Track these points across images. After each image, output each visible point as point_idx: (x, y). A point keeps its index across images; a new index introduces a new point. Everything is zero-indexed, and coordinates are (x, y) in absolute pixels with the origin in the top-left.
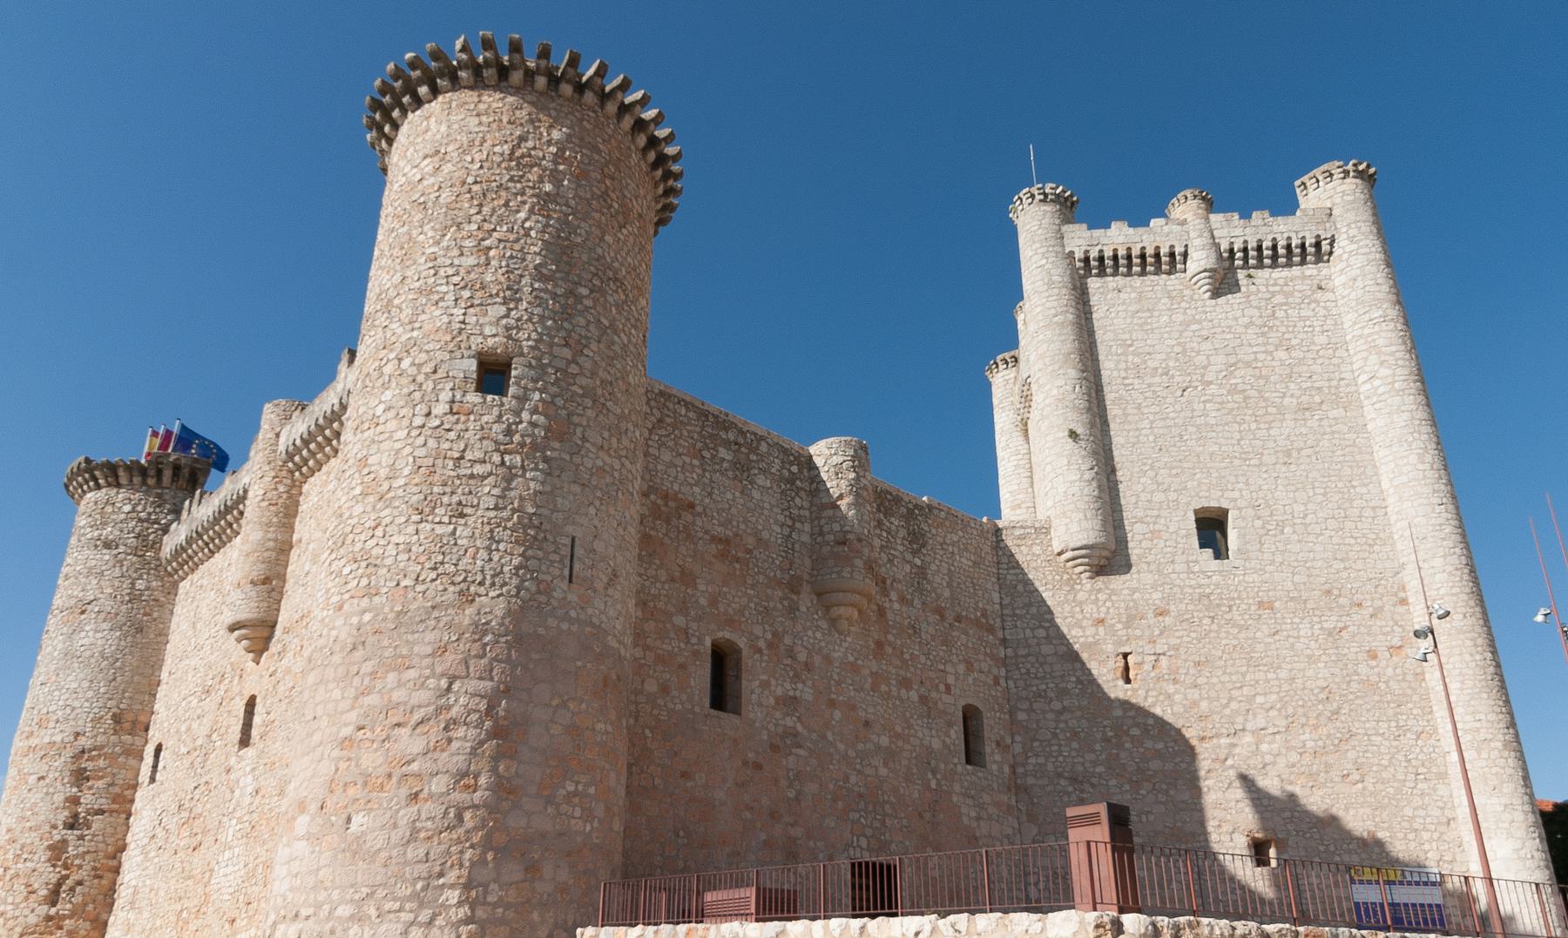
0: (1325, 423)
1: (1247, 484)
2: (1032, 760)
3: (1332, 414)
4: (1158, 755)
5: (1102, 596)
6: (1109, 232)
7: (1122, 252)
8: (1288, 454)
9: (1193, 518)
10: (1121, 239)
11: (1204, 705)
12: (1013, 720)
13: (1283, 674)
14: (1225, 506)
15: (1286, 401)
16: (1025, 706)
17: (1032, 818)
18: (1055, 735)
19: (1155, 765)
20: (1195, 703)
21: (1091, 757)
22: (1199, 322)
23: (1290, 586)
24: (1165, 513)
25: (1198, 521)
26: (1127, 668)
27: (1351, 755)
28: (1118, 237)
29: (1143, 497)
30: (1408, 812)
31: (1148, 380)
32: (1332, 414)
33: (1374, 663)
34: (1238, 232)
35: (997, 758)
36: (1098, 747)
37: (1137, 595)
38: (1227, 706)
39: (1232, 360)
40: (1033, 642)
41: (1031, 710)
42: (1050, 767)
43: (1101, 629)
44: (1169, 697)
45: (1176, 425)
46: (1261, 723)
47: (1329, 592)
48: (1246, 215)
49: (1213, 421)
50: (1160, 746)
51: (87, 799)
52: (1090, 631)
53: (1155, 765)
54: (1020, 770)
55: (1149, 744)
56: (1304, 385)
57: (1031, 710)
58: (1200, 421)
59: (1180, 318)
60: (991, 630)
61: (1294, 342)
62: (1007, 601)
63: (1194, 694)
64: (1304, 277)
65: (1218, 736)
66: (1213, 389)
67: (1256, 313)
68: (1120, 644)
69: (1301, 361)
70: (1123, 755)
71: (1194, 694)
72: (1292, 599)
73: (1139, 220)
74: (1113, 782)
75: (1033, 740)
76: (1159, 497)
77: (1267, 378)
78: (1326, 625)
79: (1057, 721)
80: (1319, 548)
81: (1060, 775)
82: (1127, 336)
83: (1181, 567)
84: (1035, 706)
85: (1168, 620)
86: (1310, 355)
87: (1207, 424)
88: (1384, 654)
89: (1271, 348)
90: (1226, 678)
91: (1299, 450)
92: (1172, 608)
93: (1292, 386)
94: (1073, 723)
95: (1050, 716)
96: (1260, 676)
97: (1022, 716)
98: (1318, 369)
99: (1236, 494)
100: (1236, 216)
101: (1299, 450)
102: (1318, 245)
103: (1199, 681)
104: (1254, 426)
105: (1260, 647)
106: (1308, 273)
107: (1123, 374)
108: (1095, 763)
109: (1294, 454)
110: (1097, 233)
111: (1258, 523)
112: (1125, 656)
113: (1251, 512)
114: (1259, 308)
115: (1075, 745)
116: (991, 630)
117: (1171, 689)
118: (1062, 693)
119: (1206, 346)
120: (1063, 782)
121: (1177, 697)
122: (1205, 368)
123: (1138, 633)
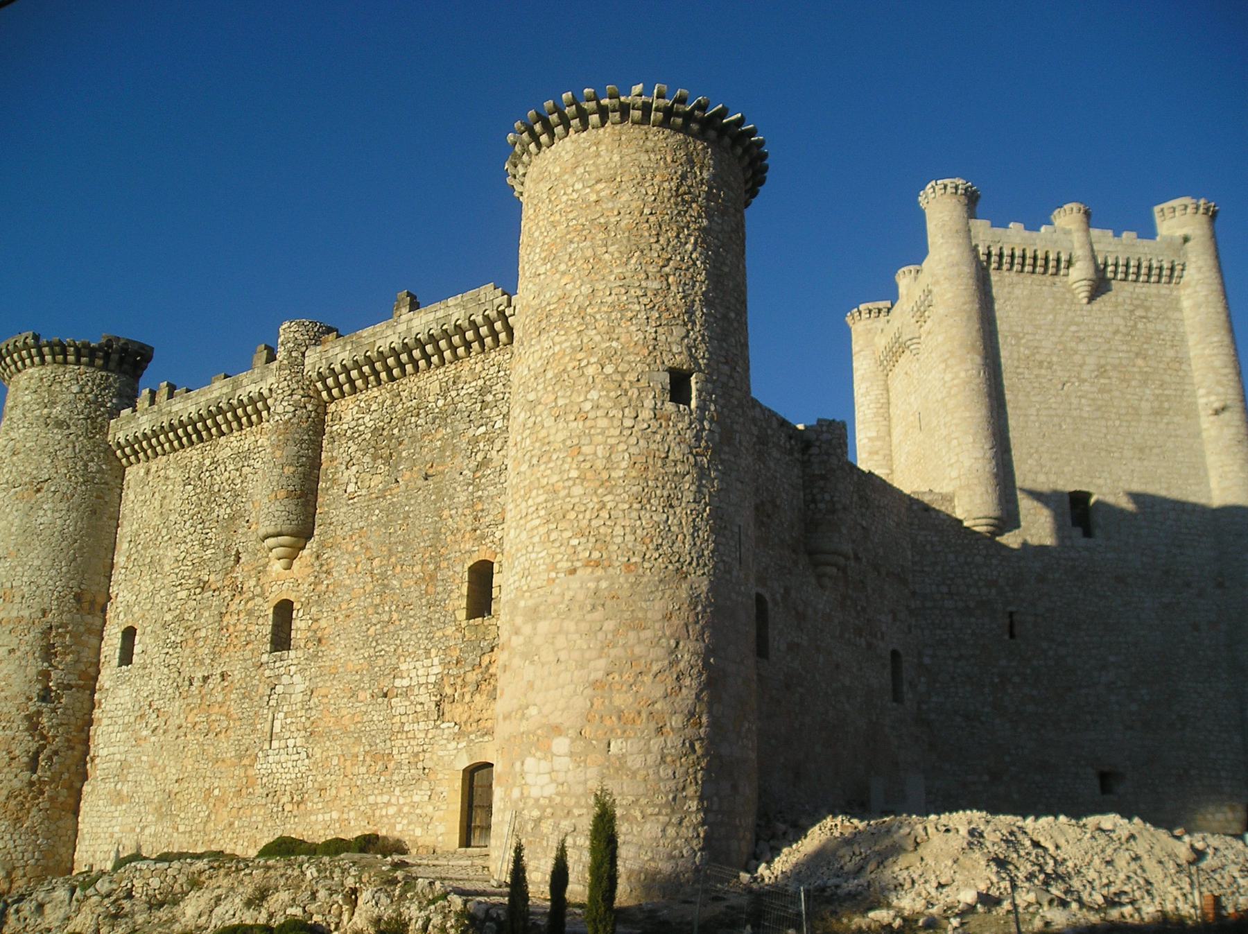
0: (1171, 427)
1: (1110, 473)
2: (934, 699)
3: (1176, 419)
15: (1143, 404)
18: (953, 678)
22: (1077, 324)
26: (1011, 626)
33: (1196, 634)
35: (910, 696)
36: (986, 690)
43: (994, 591)
45: (1057, 415)
49: (1086, 415)
50: (1035, 693)
52: (985, 591)
54: (924, 707)
56: (1157, 392)
58: (1075, 413)
64: (1159, 296)
66: (1086, 387)
73: (1033, 225)
82: (1019, 329)
86: (1161, 366)
87: (1081, 417)
90: (1086, 639)
91: (1151, 448)
92: (1050, 576)
93: (1148, 391)
97: (927, 660)
99: (1101, 482)
100: (1110, 233)
101: (1151, 448)
102: (1172, 269)
104: (1117, 423)
106: (1163, 291)
107: (1016, 363)
109: (1147, 451)
112: (1011, 614)
114: (1124, 318)
117: (1045, 645)
121: (1051, 653)
122: (1081, 366)
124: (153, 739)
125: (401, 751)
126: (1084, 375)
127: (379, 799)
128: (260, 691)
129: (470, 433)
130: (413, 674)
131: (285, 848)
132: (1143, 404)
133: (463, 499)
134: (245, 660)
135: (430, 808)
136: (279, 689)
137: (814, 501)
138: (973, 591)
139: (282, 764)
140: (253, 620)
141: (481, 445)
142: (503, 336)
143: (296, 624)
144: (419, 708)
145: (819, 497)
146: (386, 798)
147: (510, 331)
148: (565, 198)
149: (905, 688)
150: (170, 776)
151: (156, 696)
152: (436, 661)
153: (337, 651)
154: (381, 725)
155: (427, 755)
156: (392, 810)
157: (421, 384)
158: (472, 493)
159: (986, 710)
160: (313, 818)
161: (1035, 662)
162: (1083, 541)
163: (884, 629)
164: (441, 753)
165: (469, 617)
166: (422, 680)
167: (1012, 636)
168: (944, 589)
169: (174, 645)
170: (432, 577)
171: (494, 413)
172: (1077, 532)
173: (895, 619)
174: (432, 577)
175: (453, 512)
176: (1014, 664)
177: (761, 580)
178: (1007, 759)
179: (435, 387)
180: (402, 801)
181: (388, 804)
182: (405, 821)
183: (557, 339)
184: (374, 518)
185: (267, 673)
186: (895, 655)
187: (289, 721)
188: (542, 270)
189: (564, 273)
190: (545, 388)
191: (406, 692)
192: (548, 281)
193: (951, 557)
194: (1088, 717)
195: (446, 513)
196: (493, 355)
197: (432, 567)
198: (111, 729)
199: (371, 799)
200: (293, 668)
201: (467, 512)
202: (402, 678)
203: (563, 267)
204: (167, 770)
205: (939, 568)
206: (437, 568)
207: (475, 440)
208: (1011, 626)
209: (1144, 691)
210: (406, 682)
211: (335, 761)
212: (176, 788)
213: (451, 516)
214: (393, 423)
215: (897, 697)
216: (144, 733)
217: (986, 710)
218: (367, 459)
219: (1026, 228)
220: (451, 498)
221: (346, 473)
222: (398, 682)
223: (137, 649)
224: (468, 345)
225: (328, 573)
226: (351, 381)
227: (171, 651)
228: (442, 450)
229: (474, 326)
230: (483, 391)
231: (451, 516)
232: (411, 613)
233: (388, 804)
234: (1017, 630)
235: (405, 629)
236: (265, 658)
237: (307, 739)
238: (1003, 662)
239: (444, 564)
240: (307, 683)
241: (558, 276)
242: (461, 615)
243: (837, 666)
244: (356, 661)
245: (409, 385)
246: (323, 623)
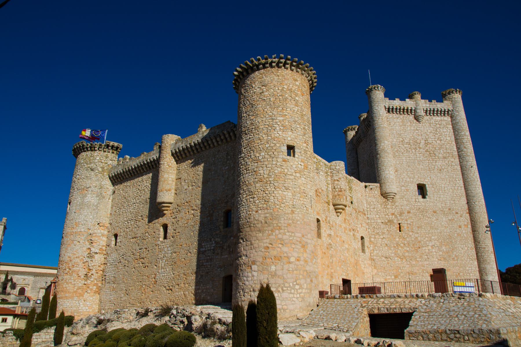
1: (430, 177)
2: (375, 252)
4: (407, 251)
5: (393, 207)
6: (395, 101)
7: (398, 108)
8: (440, 170)
9: (416, 186)
10: (398, 104)
11: (419, 238)
12: (370, 241)
13: (438, 231)
14: (424, 183)
15: (440, 155)
16: (373, 236)
17: (375, 268)
18: (381, 245)
19: (407, 254)
20: (417, 238)
21: (390, 251)
23: (440, 207)
24: (410, 184)
25: (418, 186)
26: (400, 228)
27: (455, 253)
28: (397, 103)
29: (404, 179)
30: (467, 268)
31: (405, 146)
32: (451, 160)
34: (428, 105)
37: (403, 207)
38: (424, 239)
39: (426, 142)
40: (375, 219)
41: (375, 238)
42: (380, 254)
43: (393, 216)
44: (410, 236)
46: (433, 244)
47: (450, 209)
48: (430, 101)
50: (408, 249)
51: (93, 249)
52: (391, 216)
53: (407, 254)
54: (372, 254)
55: (405, 248)
56: (445, 151)
57: (375, 238)
58: (418, 159)
59: (413, 128)
60: (365, 214)
61: (442, 138)
62: (368, 206)
63: (416, 235)
64: (444, 120)
65: (423, 247)
66: (421, 150)
67: (432, 129)
68: (398, 220)
69: (444, 144)
70: (399, 251)
71: (416, 235)
72: (442, 211)
73: (403, 99)
74: (396, 258)
75: (376, 246)
76: (408, 180)
77: (435, 148)
78: (449, 218)
79: (382, 241)
80: (448, 197)
81: (382, 256)
83: (413, 200)
84: (376, 237)
85: (411, 215)
88: (463, 227)
89: (436, 140)
91: (443, 169)
93: (441, 151)
94: (386, 242)
95: (380, 240)
96: (433, 231)
97: (372, 239)
98: (448, 147)
100: (427, 101)
101: (443, 169)
103: (419, 232)
105: (433, 223)
108: (391, 253)
110: (391, 101)
111: (433, 189)
112: (399, 224)
113: (431, 186)
115: (386, 248)
116: (365, 214)
117: (411, 233)
118: (383, 233)
119: (420, 138)
120: (383, 258)
121: (413, 236)
123: (403, 218)
126: (421, 146)
132: (440, 155)
135: (212, 290)
137: (334, 188)
138: (387, 216)
142: (233, 138)
145: (336, 187)
147: (235, 135)
149: (366, 248)
159: (393, 255)
161: (408, 239)
162: (422, 200)
163: (358, 229)
167: (400, 231)
168: (378, 216)
172: (421, 196)
173: (362, 226)
176: (401, 240)
177: (318, 214)
178: (400, 271)
186: (362, 238)
193: (379, 206)
194: (426, 257)
205: (375, 210)
208: (400, 228)
209: (444, 248)
215: (363, 250)
217: (393, 255)
219: (400, 100)
224: (222, 140)
234: (402, 228)
238: (397, 240)
243: (344, 242)
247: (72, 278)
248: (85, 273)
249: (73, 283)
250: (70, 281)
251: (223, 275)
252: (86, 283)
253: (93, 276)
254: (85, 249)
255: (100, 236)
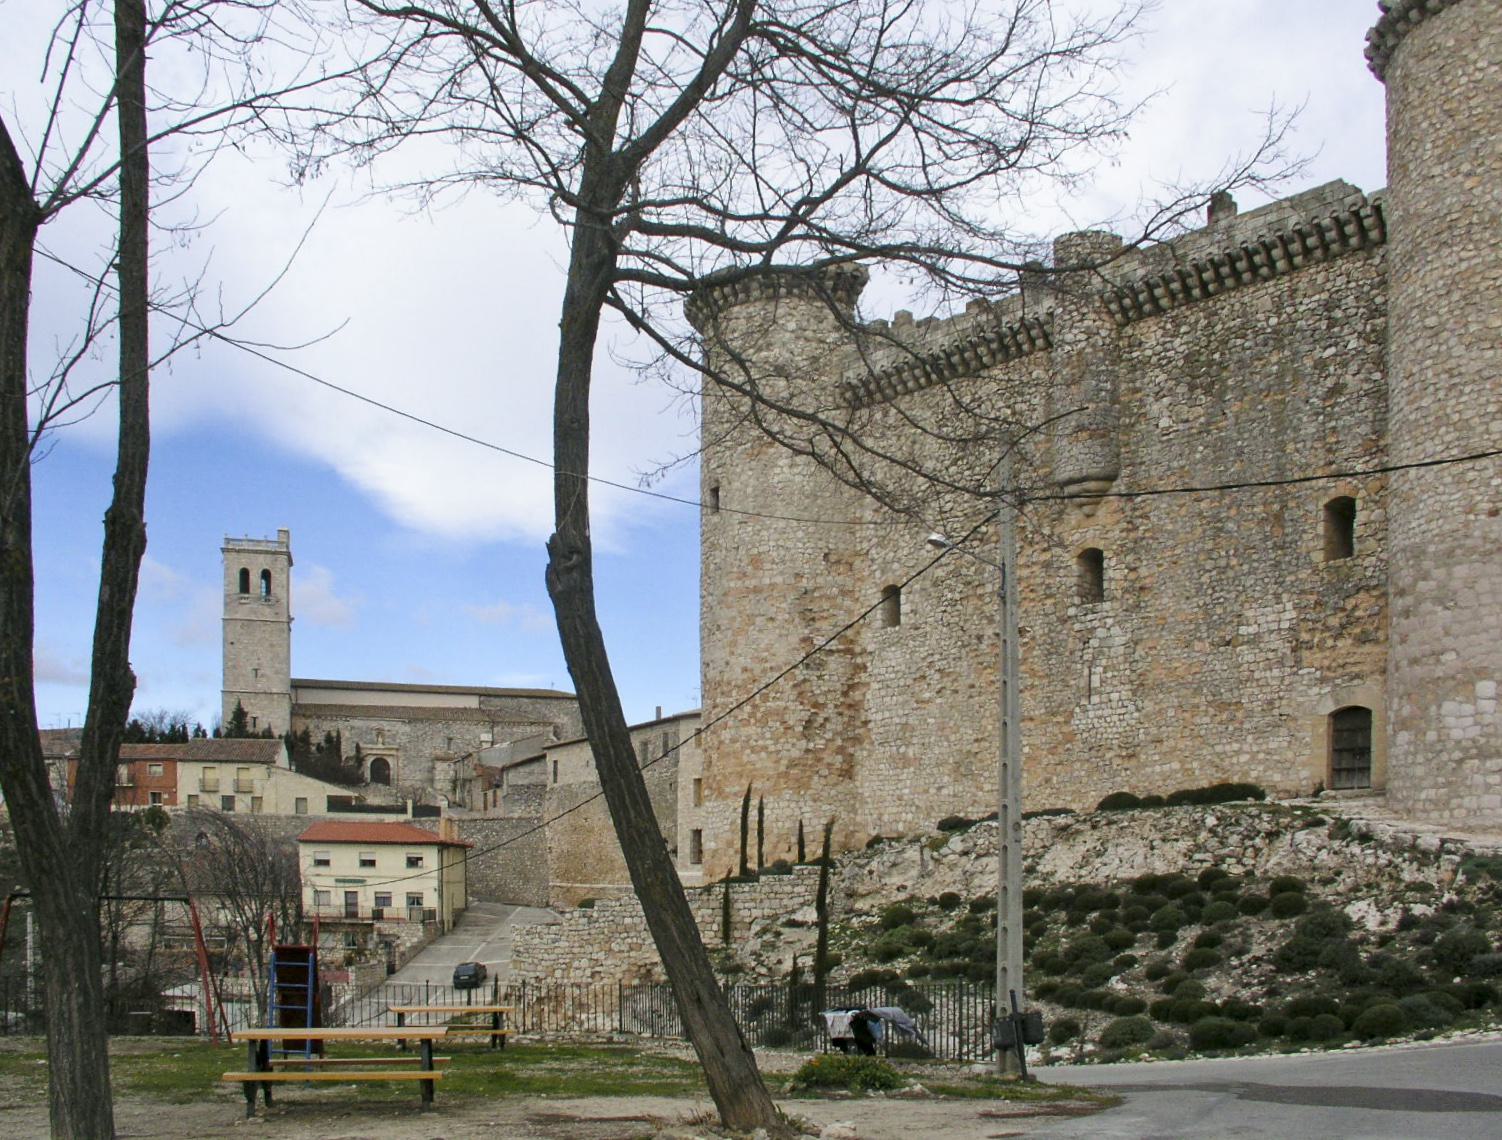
124: (939, 701)
125: (1252, 697)
127: (1228, 748)
128: (1070, 646)
129: (1317, 353)
130: (1261, 620)
131: (1119, 802)
133: (1311, 430)
134: (1046, 615)
136: (1094, 643)
139: (1109, 714)
140: (1052, 572)
141: (1332, 369)
143: (1109, 574)
144: (1271, 655)
146: (1236, 746)
148: (1464, 80)
150: (966, 737)
151: (937, 657)
152: (1289, 606)
153: (1165, 601)
154: (1225, 675)
155: (1284, 702)
156: (1244, 758)
157: (1246, 299)
158: (1324, 423)
160: (1149, 770)
164: (1301, 699)
165: (1327, 560)
166: (1274, 626)
169: (953, 603)
170: (1278, 518)
171: (1346, 331)
174: (1278, 518)
175: (1300, 445)
179: (1267, 302)
180: (1255, 749)
181: (1238, 753)
182: (1261, 768)
183: (1463, 254)
184: (1198, 456)
185: (1077, 626)
187: (1109, 675)
188: (1436, 171)
189: (1468, 175)
190: (1451, 312)
191: (1254, 640)
192: (1446, 184)
195: (1290, 447)
196: (1340, 262)
197: (1276, 507)
198: (883, 693)
199: (1219, 748)
200: (1110, 621)
201: (1318, 445)
202: (1248, 625)
203: (1465, 168)
204: (962, 730)
206: (1284, 507)
207: (1321, 365)
210: (1252, 629)
211: (1171, 713)
212: (975, 748)
213: (1297, 450)
214: (1213, 346)
216: (927, 695)
218: (1182, 389)
220: (1296, 429)
221: (1155, 407)
222: (1243, 630)
223: (905, 608)
225: (1146, 516)
226: (1154, 300)
227: (949, 609)
228: (1280, 375)
229: (1320, 230)
230: (1329, 306)
231: (1297, 450)
232: (1255, 557)
233: (1238, 753)
235: (1249, 573)
236: (1072, 611)
237: (1134, 692)
239: (1291, 504)
240: (1129, 635)
241: (1460, 178)
242: (1318, 557)
244: (1190, 609)
245: (1229, 305)
246: (1143, 572)
247: (768, 735)
248: (805, 715)
249: (772, 748)
250: (761, 743)
251: (1330, 707)
252: (811, 745)
253: (828, 726)
254: (794, 640)
255: (835, 598)
